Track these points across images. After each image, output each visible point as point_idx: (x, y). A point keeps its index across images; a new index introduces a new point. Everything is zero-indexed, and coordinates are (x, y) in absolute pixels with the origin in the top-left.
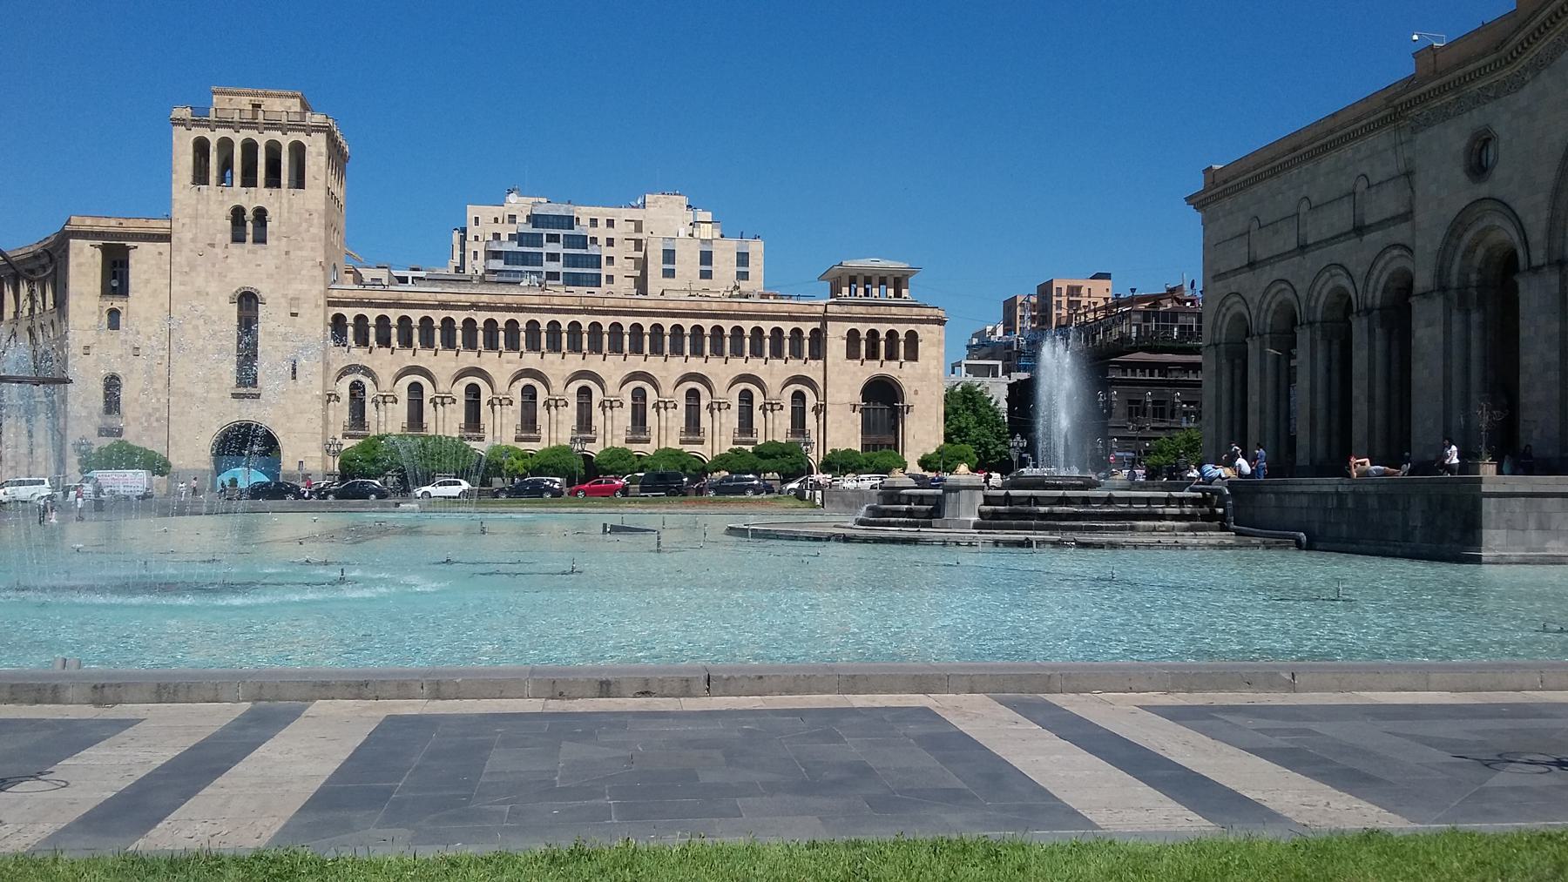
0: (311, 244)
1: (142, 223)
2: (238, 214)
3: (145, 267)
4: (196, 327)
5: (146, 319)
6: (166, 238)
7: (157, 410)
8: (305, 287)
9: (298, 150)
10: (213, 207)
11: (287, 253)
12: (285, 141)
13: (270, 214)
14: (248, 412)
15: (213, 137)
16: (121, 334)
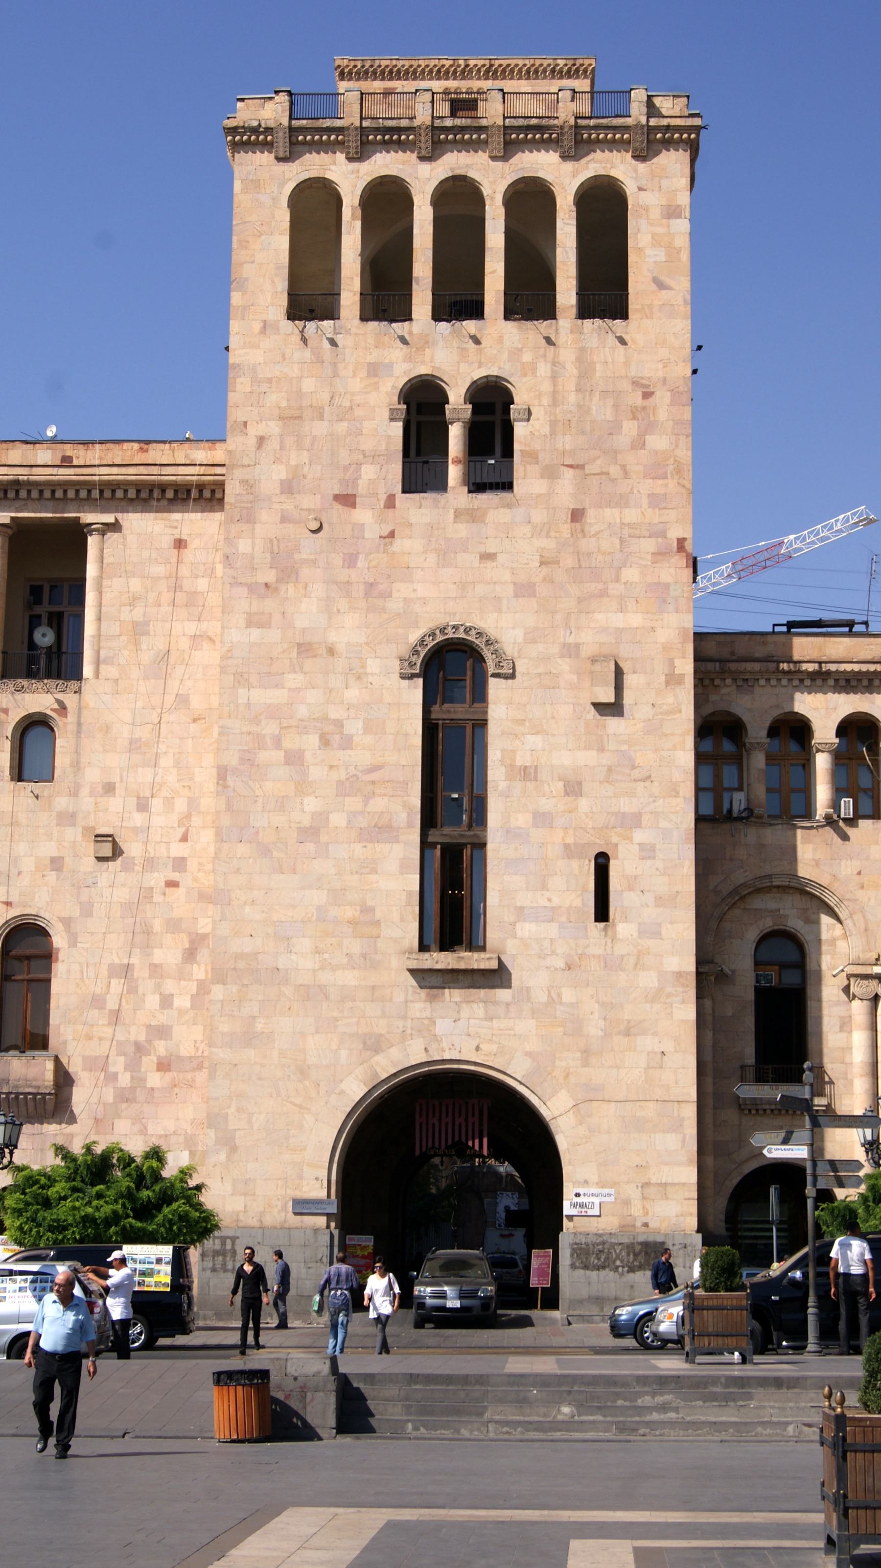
0: (646, 487)
1: (118, 454)
2: (422, 403)
3: (135, 585)
4: (294, 759)
5: (134, 745)
6: (205, 495)
7: (162, 1032)
8: (635, 620)
9: (604, 209)
10: (354, 383)
11: (577, 515)
12: (565, 177)
13: (521, 398)
14: (464, 1034)
15: (350, 178)
16: (57, 796)
